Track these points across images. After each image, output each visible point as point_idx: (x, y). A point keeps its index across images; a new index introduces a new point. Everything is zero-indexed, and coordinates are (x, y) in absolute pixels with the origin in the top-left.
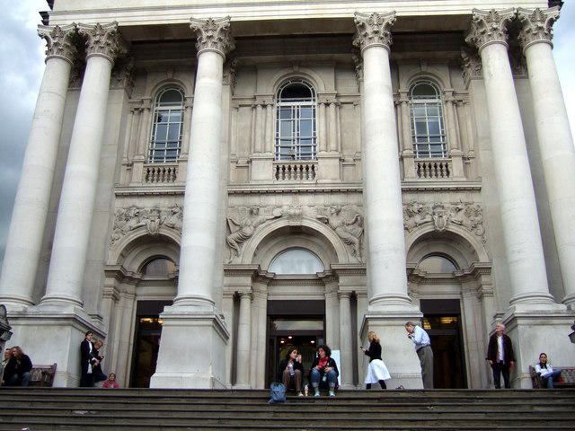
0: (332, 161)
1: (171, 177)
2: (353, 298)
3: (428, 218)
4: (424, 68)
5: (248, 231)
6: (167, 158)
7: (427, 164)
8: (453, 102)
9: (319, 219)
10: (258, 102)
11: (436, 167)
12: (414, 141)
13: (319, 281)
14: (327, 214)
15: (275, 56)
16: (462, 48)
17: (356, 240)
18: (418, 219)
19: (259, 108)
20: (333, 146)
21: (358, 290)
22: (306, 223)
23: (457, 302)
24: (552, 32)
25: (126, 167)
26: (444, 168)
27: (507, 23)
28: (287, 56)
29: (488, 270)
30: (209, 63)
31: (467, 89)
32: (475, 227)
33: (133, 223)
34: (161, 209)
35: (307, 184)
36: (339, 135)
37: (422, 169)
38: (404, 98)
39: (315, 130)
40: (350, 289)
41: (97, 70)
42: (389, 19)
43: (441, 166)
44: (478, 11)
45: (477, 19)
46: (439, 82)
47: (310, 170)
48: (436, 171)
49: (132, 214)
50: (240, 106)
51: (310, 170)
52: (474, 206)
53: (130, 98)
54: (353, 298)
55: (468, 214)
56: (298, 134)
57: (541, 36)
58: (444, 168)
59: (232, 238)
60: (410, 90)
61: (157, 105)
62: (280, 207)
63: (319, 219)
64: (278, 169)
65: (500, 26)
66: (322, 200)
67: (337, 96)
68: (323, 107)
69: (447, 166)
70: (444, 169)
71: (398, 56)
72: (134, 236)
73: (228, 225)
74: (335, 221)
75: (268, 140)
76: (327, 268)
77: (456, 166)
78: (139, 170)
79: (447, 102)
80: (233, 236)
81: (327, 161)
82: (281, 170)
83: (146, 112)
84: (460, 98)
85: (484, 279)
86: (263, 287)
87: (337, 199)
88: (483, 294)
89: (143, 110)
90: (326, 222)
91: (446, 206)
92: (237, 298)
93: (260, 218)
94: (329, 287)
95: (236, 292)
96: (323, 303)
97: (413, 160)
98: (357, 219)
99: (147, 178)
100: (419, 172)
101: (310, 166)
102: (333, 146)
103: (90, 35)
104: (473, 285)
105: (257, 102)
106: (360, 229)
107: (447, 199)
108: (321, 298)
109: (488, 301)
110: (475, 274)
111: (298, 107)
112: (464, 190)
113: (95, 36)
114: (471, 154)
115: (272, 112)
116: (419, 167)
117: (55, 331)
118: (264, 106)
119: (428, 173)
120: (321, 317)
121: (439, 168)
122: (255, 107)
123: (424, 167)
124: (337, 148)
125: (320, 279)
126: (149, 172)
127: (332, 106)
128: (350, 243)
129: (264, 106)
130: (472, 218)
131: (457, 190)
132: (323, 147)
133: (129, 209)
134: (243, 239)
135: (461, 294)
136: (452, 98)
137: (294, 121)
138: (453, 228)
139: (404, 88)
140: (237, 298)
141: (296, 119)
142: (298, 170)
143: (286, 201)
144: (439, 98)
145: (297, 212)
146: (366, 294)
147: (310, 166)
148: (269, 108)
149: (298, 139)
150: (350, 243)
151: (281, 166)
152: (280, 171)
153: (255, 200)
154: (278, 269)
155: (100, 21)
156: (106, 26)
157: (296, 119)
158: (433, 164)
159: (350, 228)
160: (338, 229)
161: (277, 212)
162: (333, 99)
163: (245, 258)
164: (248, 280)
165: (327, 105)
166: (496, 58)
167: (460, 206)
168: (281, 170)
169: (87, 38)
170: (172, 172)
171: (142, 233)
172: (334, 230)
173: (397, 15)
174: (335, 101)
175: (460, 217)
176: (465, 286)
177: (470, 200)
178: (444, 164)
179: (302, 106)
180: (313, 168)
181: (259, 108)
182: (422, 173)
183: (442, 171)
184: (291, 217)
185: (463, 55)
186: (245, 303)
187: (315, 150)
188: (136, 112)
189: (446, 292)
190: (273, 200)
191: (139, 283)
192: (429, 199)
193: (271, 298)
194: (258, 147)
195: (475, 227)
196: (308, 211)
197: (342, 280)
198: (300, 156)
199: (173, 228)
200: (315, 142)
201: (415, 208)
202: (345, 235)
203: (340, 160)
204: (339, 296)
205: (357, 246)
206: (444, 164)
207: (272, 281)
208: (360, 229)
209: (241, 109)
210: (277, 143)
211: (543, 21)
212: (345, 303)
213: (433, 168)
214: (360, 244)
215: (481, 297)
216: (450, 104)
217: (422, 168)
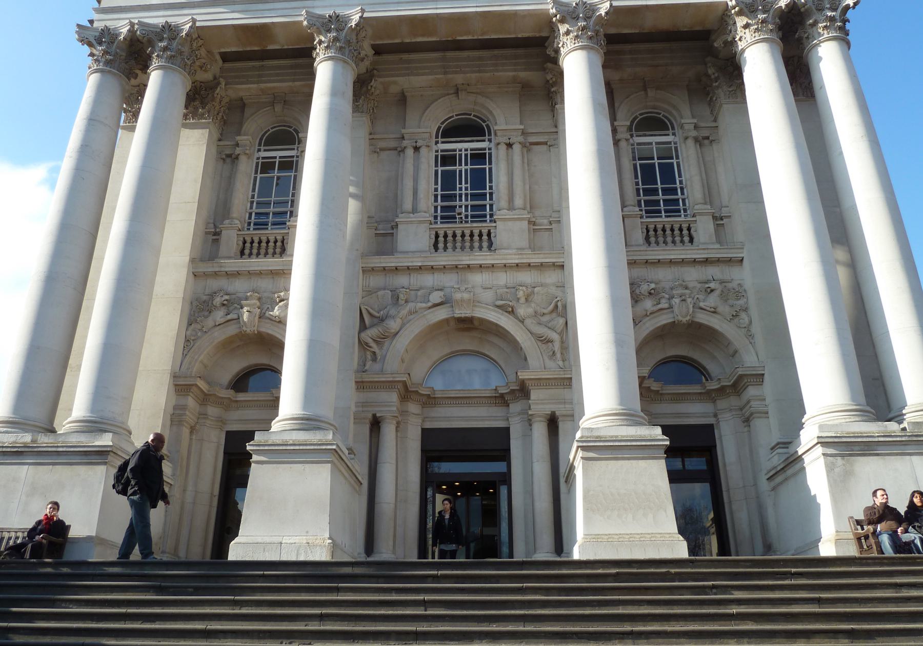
0: (518, 223)
1: (278, 250)
2: (553, 423)
3: (664, 304)
4: (651, 93)
6: (274, 224)
7: (660, 227)
8: (696, 140)
9: (499, 307)
11: (672, 230)
12: (639, 195)
13: (501, 400)
15: (430, 77)
16: (709, 59)
17: (555, 336)
18: (648, 304)
19: (410, 152)
21: (560, 410)
24: (848, 26)
25: (211, 237)
26: (685, 232)
28: (450, 76)
31: (715, 121)
32: (735, 316)
35: (482, 257)
36: (527, 187)
37: (651, 236)
38: (623, 134)
39: (491, 181)
40: (548, 409)
43: (681, 230)
46: (674, 112)
47: (485, 237)
48: (673, 236)
49: (218, 301)
50: (382, 149)
51: (485, 237)
52: (734, 285)
53: (220, 140)
54: (553, 423)
55: (724, 297)
56: (466, 189)
58: (685, 232)
60: (632, 122)
61: (259, 150)
63: (499, 307)
64: (437, 236)
66: (502, 279)
67: (524, 133)
68: (503, 148)
69: (689, 229)
71: (616, 76)
74: (522, 311)
75: (421, 195)
76: (512, 378)
77: (704, 229)
78: (231, 239)
79: (686, 138)
81: (510, 223)
82: (441, 239)
83: (243, 158)
84: (705, 133)
85: (752, 391)
86: (413, 408)
87: (526, 277)
88: (752, 414)
89: (237, 158)
90: (512, 312)
91: (691, 285)
92: (376, 424)
94: (515, 407)
95: (374, 416)
96: (507, 430)
97: (639, 220)
98: (556, 306)
99: (242, 253)
100: (647, 239)
101: (485, 232)
102: (518, 202)
104: (733, 401)
105: (405, 143)
106: (561, 321)
107: (692, 275)
108: (500, 424)
109: (758, 424)
110: (737, 386)
111: (466, 150)
112: (718, 261)
113: (161, 40)
114: (725, 211)
115: (428, 159)
116: (648, 231)
117: (82, 470)
118: (417, 149)
119: (661, 239)
120: (504, 455)
121: (677, 232)
122: (403, 150)
123: (655, 230)
124: (525, 204)
125: (502, 396)
126: (245, 242)
127: (517, 148)
129: (417, 149)
130: (731, 302)
131: (706, 262)
132: (504, 203)
133: (212, 295)
135: (715, 415)
136: (694, 133)
137: (461, 171)
138: (703, 318)
139: (623, 122)
141: (463, 167)
142: (467, 238)
143: (448, 280)
144: (674, 134)
146: (573, 416)
147: (485, 232)
148: (423, 151)
149: (466, 195)
151: (441, 233)
153: (402, 280)
155: (170, 20)
157: (463, 167)
158: (668, 227)
159: (545, 319)
160: (528, 322)
161: (436, 297)
162: (516, 138)
164: (393, 397)
165: (509, 145)
167: (712, 285)
168: (441, 239)
170: (279, 244)
174: (521, 139)
175: (712, 301)
176: (722, 404)
177: (727, 277)
178: (685, 226)
179: (471, 150)
180: (489, 234)
181: (410, 152)
182: (653, 239)
183: (682, 236)
185: (710, 71)
186: (389, 432)
187: (491, 209)
188: (228, 160)
190: (428, 280)
191: (228, 405)
192: (664, 275)
193: (428, 425)
194: (408, 205)
197: (535, 395)
198: (469, 219)
200: (491, 199)
201: (645, 288)
203: (530, 222)
205: (557, 346)
206: (685, 226)
207: (430, 401)
208: (561, 321)
209: (384, 155)
210: (436, 200)
211: (835, 10)
212: (540, 431)
213: (668, 232)
214: (562, 342)
215: (747, 421)
216: (690, 142)
217: (652, 233)
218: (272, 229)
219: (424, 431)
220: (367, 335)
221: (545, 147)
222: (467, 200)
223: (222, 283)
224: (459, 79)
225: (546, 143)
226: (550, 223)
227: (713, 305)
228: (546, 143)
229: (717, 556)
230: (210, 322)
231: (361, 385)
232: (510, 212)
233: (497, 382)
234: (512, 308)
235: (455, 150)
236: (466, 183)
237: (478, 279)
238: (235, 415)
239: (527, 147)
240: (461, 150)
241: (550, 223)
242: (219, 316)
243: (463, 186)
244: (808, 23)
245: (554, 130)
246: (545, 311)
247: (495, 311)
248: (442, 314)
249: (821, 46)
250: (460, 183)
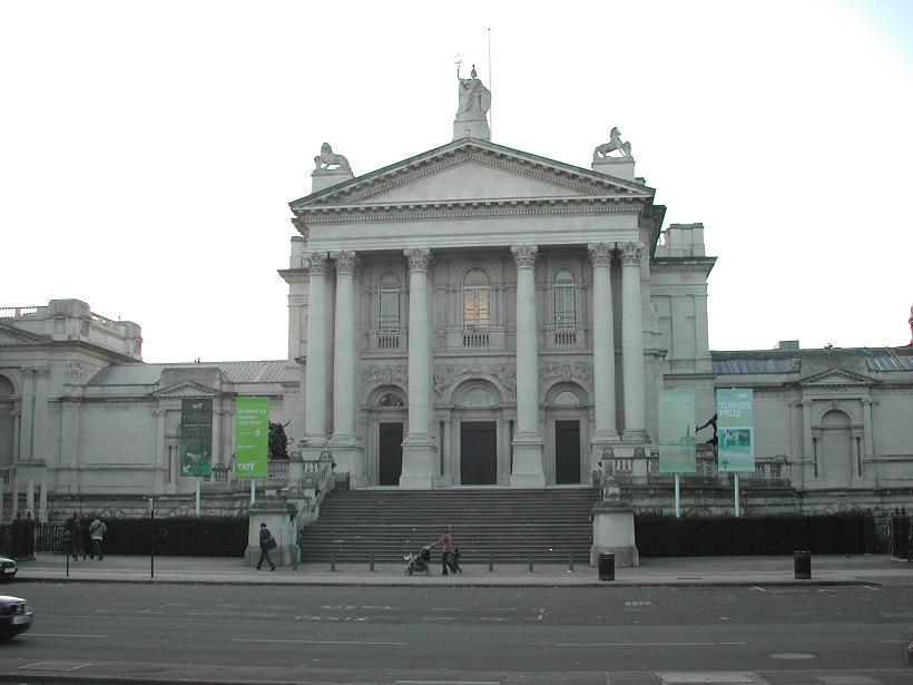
5: (447, 383)
10: (450, 288)
13: (493, 410)
20: (501, 322)
23: (578, 422)
29: (593, 407)
30: (418, 280)
33: (374, 378)
35: (483, 350)
41: (345, 283)
59: (437, 387)
62: (466, 366)
65: (606, 254)
66: (493, 361)
70: (572, 337)
72: (375, 386)
73: (435, 380)
74: (500, 376)
77: (580, 336)
80: (437, 385)
85: (591, 411)
86: (458, 414)
90: (496, 376)
92: (442, 424)
93: (455, 373)
94: (498, 414)
96: (495, 423)
107: (572, 360)
133: (371, 368)
134: (447, 387)
138: (575, 380)
140: (442, 424)
143: (471, 362)
150: (510, 390)
152: (466, 340)
153: (451, 361)
154: (466, 404)
161: (465, 370)
163: (446, 400)
164: (449, 413)
166: (602, 276)
171: (380, 384)
184: (474, 373)
186: (447, 426)
189: (572, 416)
190: (462, 361)
195: (588, 379)
196: (484, 368)
202: (508, 385)
207: (464, 410)
212: (507, 426)
219: (462, 423)
220: (437, 387)
223: (374, 362)
229: (558, 482)
230: (370, 380)
231: (435, 409)
233: (492, 403)
237: (482, 361)
238: (381, 416)
239: (505, 290)
242: (374, 378)
248: (468, 377)
249: (663, 209)
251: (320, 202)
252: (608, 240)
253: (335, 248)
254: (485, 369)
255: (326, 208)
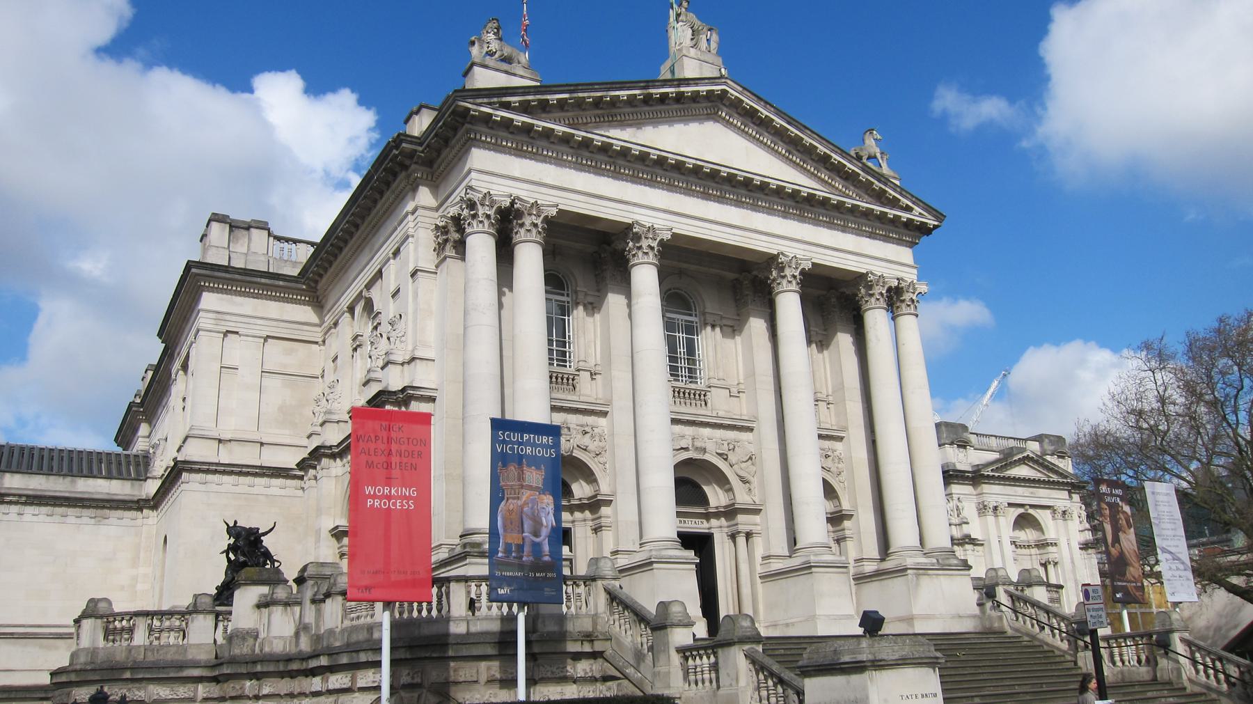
0: (723, 390)
2: (748, 535)
9: (717, 453)
14: (724, 450)
21: (754, 529)
22: (707, 457)
27: (889, 290)
34: (571, 426)
40: (747, 528)
42: (807, 265)
44: (872, 273)
45: (871, 281)
57: (912, 306)
66: (719, 433)
68: (709, 328)
74: (732, 458)
98: (750, 458)
103: (526, 212)
128: (744, 481)
130: (836, 465)
145: (703, 445)
156: (543, 205)
159: (744, 465)
169: (519, 214)
172: (732, 467)
173: (814, 260)
199: (585, 450)
202: (742, 474)
204: (733, 537)
211: (914, 293)
212: (741, 540)
218: (557, 365)
221: (730, 329)
222: (685, 364)
224: (685, 266)
225: (731, 326)
226: (739, 392)
227: (829, 466)
228: (731, 326)
232: (718, 382)
234: (727, 455)
235: (674, 319)
236: (684, 349)
240: (678, 320)
241: (739, 392)
243: (682, 350)
244: (901, 298)
245: (738, 318)
246: (744, 460)
247: (717, 457)
250: (680, 348)
251: (507, 106)
252: (891, 274)
253: (526, 194)
254: (710, 446)
255: (519, 119)
